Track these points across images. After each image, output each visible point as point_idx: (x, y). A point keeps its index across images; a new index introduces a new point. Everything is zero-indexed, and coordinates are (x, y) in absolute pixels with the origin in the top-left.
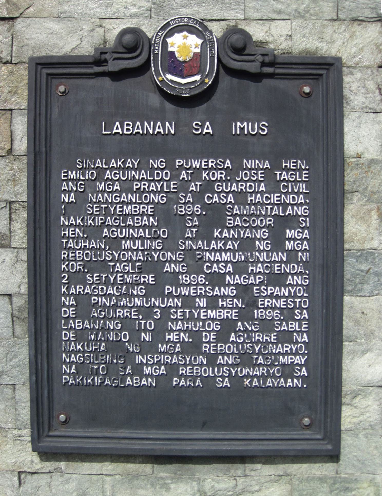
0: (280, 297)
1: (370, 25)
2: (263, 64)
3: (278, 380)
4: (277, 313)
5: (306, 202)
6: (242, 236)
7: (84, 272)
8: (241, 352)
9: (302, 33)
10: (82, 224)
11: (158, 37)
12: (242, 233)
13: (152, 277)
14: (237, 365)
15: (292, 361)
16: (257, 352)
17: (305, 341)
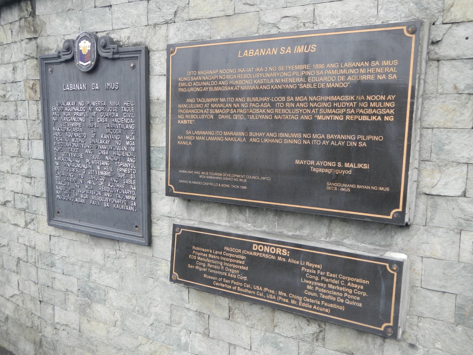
1: (162, 26)
2: (114, 53)
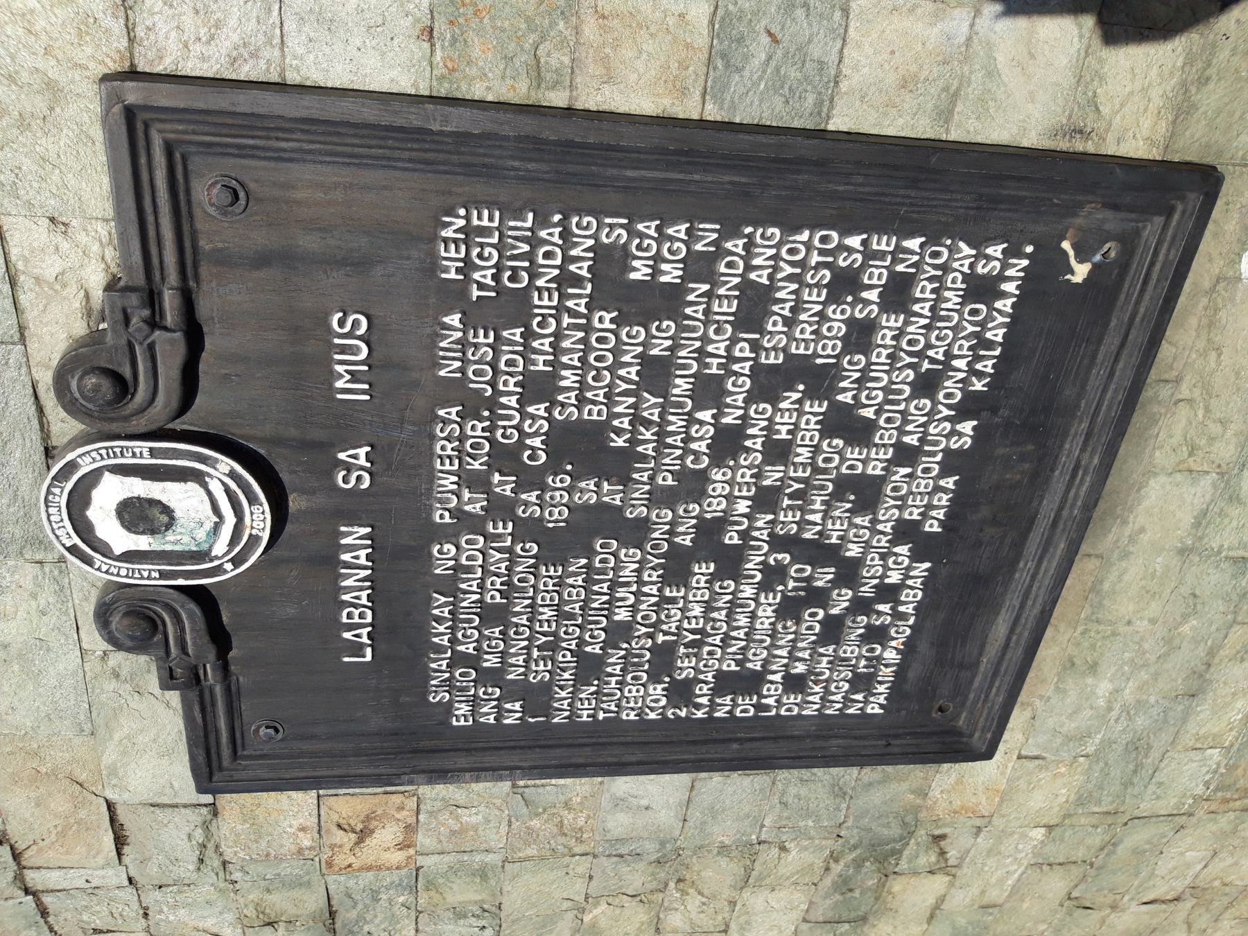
4: (834, 312)
15: (960, 277)
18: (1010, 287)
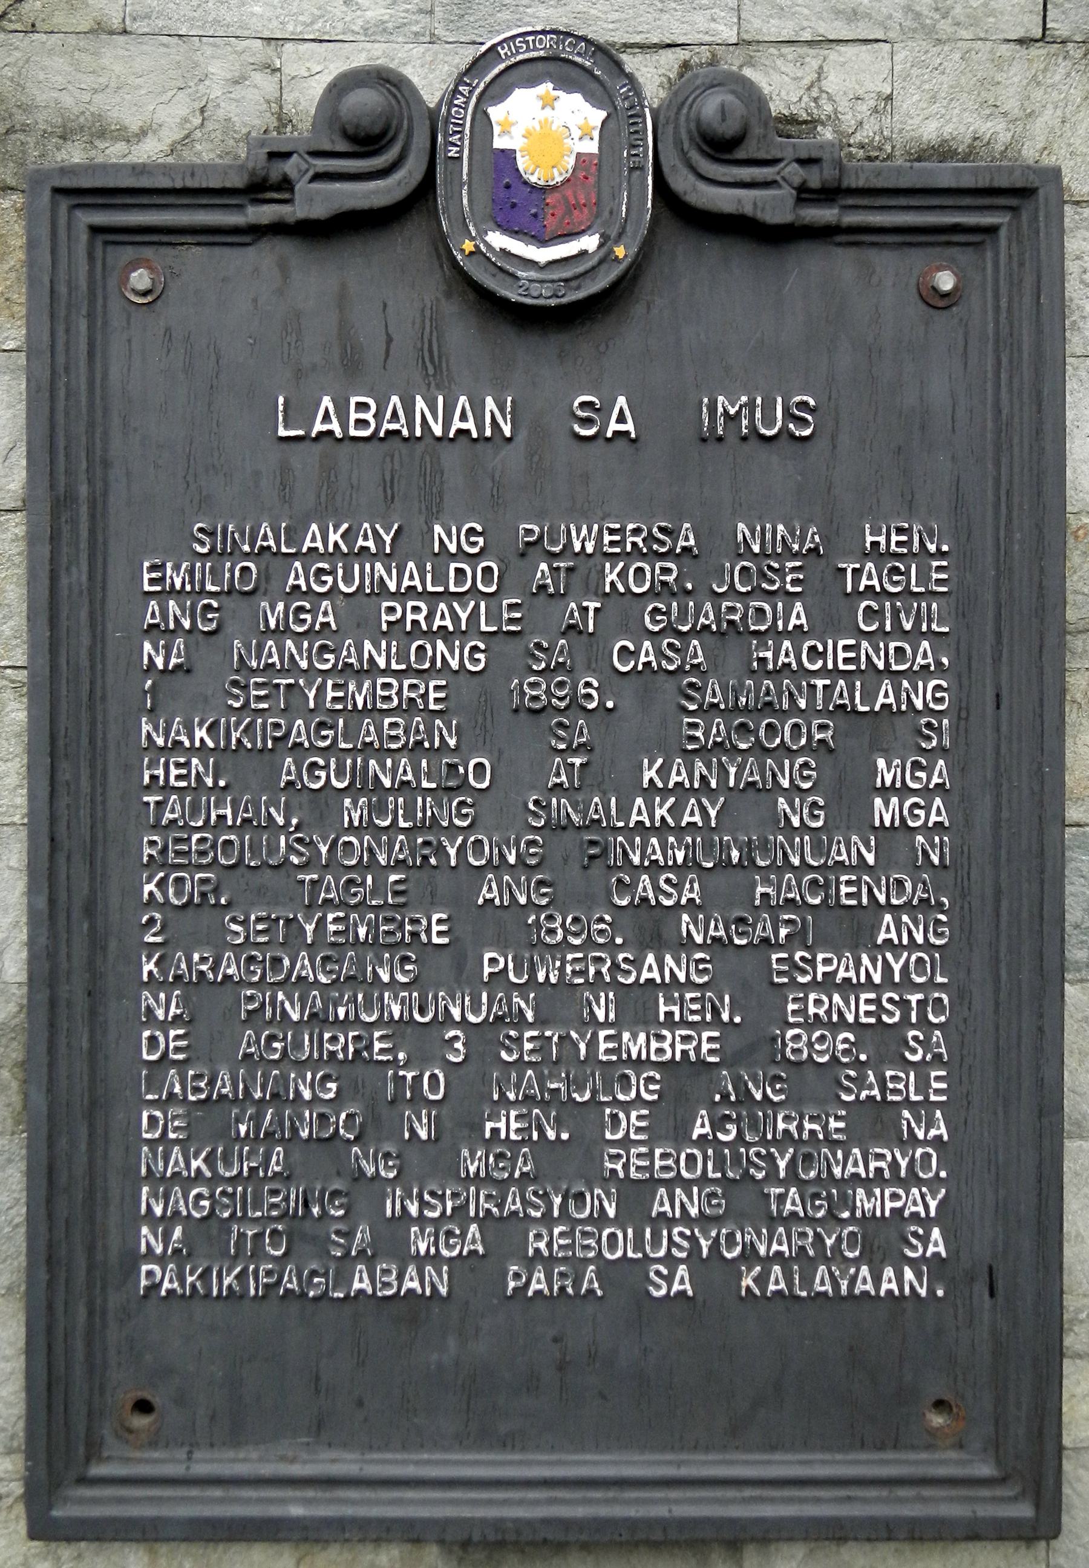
0: (858, 988)
2: (805, 195)
3: (852, 1271)
4: (846, 1040)
5: (939, 664)
6: (732, 783)
7: (217, 905)
8: (730, 1174)
9: (926, 87)
10: (211, 744)
11: (459, 101)
12: (732, 770)
13: (440, 922)
14: (716, 1220)
15: (898, 1204)
16: (782, 1174)
17: (939, 1138)
18: (889, 1284)
